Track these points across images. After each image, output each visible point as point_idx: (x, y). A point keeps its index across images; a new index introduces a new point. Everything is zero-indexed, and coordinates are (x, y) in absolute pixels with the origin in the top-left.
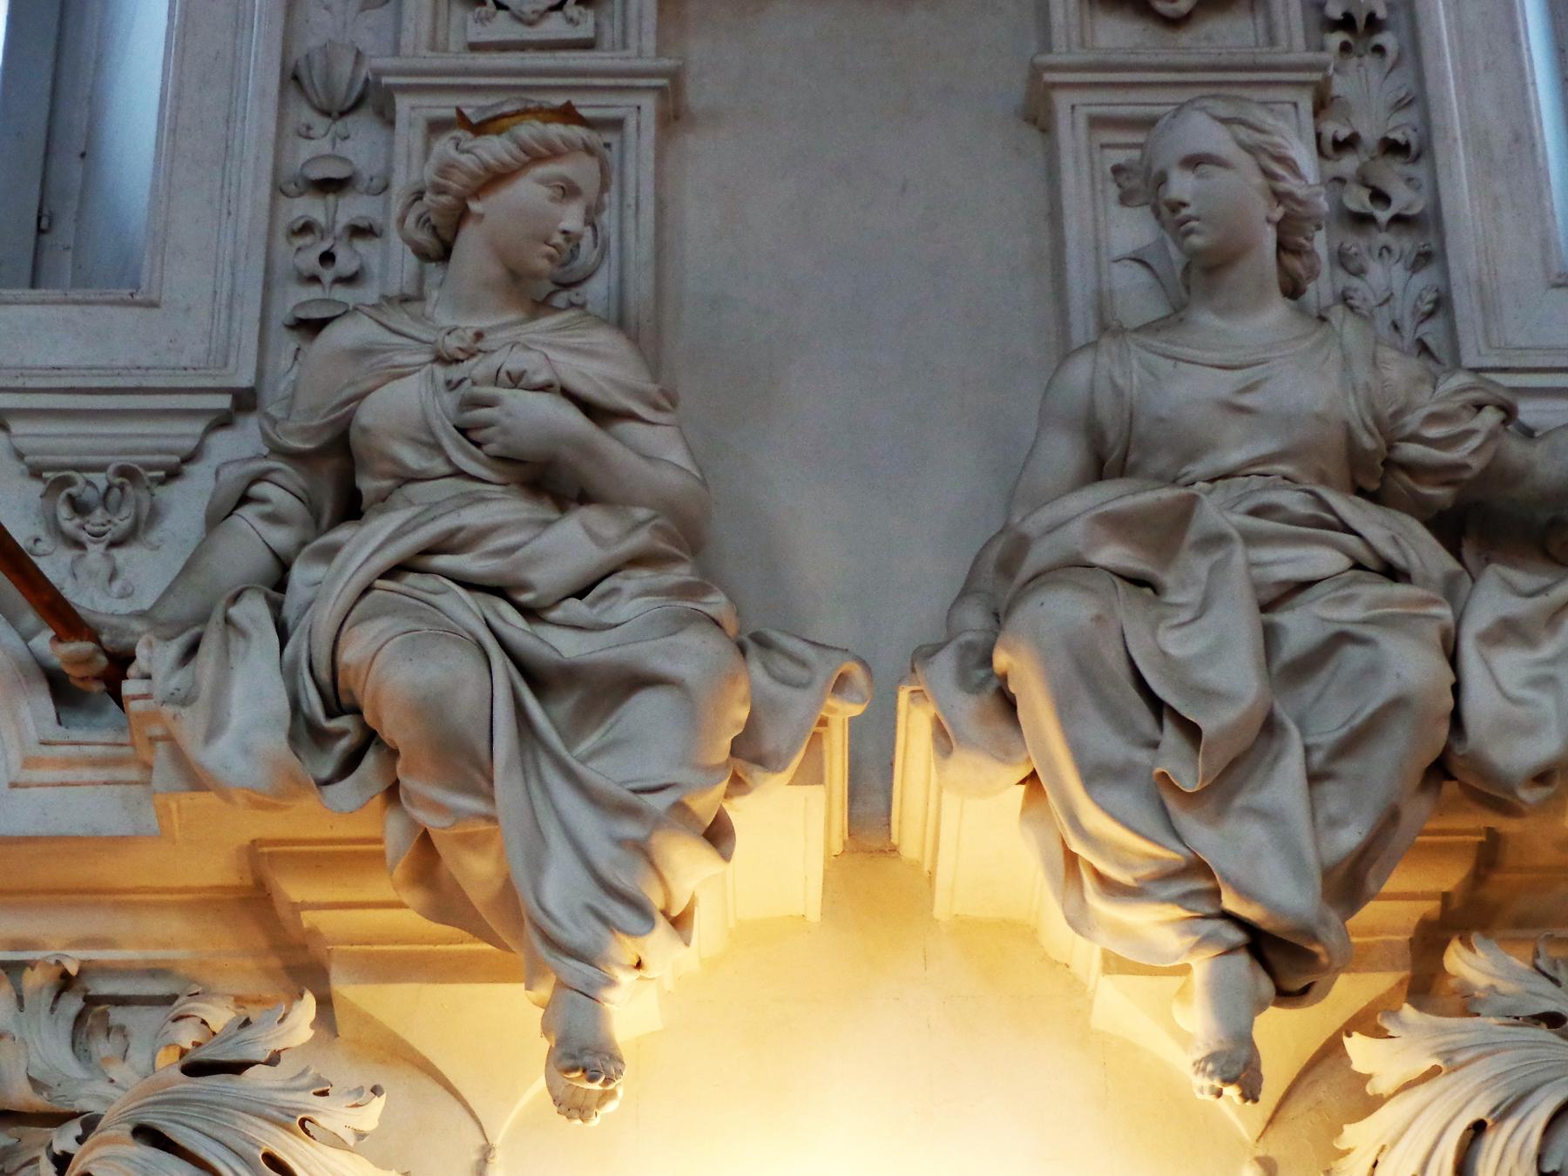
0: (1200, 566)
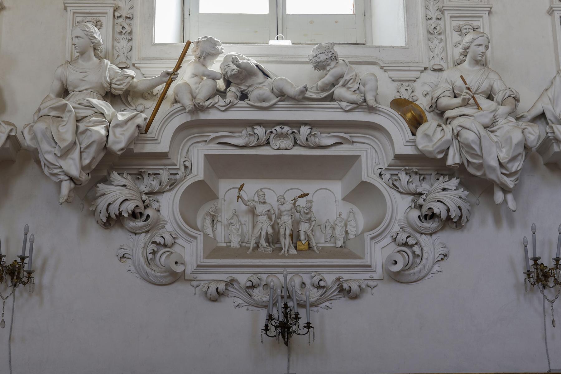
0: (68, 114)
